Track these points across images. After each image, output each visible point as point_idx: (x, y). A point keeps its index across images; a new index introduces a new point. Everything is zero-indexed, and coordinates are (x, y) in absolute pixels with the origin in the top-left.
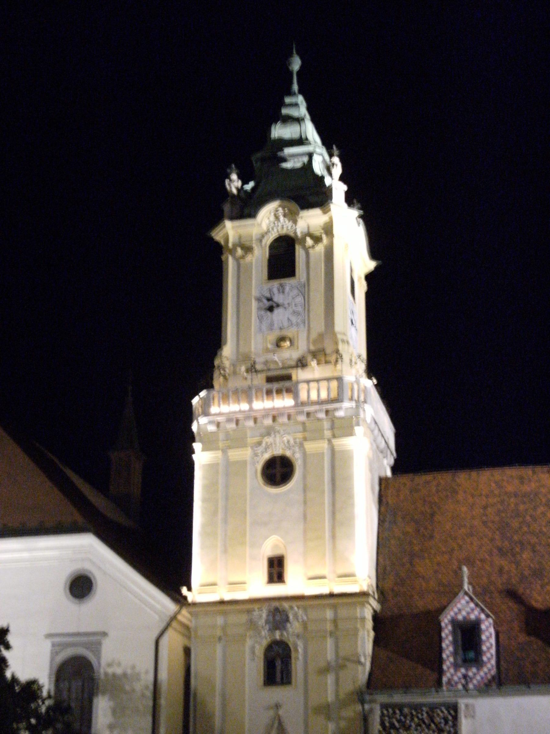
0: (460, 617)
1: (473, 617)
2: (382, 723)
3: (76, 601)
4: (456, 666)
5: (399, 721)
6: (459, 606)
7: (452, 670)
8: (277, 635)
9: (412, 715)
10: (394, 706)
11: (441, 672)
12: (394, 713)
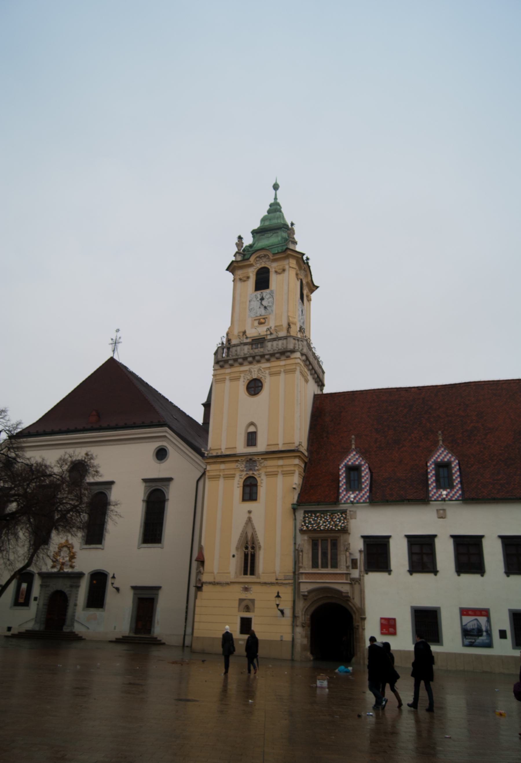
0: (350, 463)
1: (357, 463)
2: (304, 521)
3: (159, 462)
4: (347, 490)
5: (314, 520)
6: (350, 457)
7: (345, 493)
8: (250, 473)
9: (321, 516)
10: (311, 512)
11: (338, 494)
12: (311, 516)
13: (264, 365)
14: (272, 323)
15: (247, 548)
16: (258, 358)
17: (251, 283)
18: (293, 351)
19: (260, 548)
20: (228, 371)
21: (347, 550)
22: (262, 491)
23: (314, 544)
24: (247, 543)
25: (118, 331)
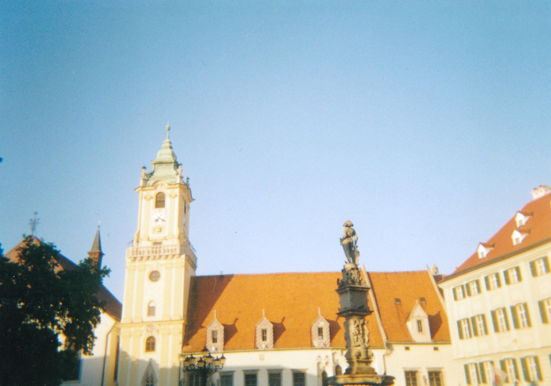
13: (162, 261)
14: (165, 233)
15: (148, 382)
16: (157, 257)
17: (153, 202)
18: (180, 255)
19: (157, 381)
20: (137, 263)
21: (211, 380)
22: (158, 345)
23: (191, 378)
24: (148, 378)
25: (36, 213)
